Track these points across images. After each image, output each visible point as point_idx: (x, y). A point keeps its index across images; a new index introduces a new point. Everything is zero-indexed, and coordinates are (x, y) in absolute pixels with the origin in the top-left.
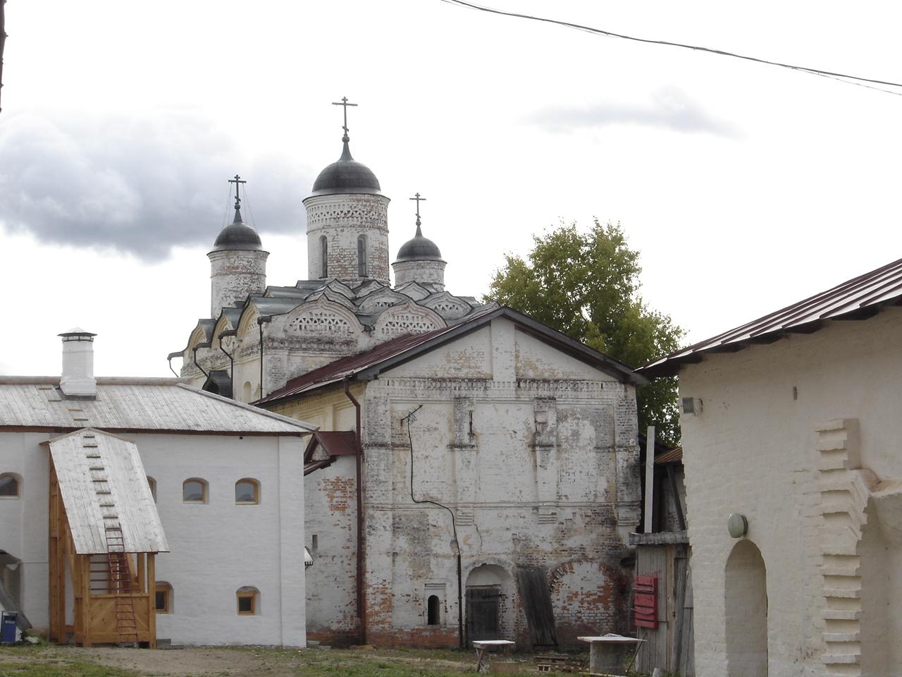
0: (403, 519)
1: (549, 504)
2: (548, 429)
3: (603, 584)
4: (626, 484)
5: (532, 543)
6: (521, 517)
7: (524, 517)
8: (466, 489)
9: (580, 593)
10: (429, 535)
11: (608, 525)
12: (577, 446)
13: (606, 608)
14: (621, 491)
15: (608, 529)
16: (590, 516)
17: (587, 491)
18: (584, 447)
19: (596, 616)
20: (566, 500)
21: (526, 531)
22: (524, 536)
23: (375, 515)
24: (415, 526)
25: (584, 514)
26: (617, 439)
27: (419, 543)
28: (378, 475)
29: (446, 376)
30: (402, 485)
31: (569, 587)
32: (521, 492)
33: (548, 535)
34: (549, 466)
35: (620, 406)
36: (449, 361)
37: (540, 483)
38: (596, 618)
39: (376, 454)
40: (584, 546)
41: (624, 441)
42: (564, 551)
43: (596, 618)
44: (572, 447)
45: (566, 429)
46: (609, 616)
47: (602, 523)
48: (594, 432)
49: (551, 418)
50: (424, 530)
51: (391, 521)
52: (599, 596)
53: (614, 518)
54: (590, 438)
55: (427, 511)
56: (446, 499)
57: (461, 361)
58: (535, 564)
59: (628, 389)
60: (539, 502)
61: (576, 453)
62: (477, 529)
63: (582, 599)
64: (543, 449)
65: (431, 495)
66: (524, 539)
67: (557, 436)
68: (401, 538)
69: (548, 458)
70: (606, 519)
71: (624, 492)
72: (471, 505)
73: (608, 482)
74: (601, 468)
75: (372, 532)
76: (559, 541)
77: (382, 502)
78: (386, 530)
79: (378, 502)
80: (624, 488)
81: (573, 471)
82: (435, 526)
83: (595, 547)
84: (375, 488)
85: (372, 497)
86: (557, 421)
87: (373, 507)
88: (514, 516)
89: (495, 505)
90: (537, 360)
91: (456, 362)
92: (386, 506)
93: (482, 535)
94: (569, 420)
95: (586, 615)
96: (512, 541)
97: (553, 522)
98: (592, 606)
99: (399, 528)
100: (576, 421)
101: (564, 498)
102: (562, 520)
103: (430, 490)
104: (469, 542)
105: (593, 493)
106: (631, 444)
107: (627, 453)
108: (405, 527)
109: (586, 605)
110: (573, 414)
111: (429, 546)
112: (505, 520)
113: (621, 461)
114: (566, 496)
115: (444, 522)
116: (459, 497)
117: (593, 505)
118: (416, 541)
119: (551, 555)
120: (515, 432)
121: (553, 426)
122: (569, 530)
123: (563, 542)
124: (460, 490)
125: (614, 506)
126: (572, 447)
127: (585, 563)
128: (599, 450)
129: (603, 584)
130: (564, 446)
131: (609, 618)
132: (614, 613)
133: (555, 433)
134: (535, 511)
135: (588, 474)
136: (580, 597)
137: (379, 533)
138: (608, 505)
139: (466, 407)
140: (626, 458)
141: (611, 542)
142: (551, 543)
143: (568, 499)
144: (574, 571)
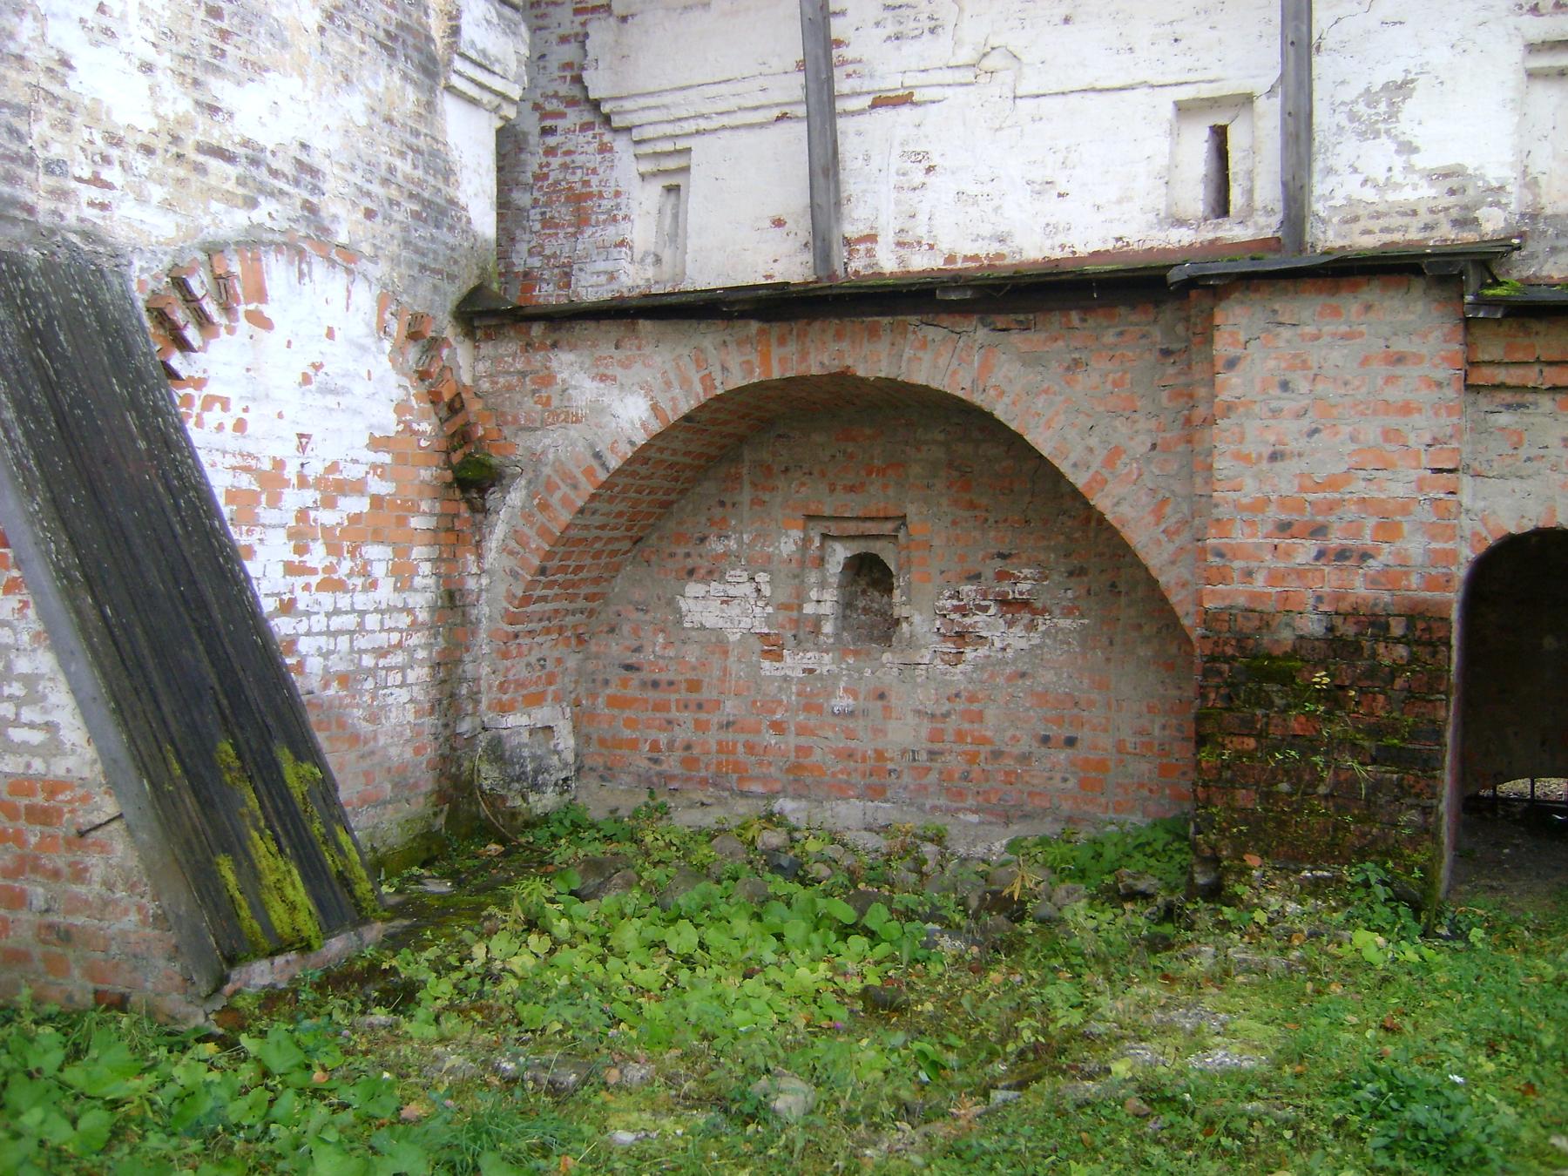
3: (390, 424)
9: (291, 472)
13: (402, 575)
19: (361, 624)
31: (240, 426)
38: (362, 643)
40: (316, 160)
42: (219, 153)
43: (362, 643)
46: (415, 626)
52: (377, 501)
58: (44, 206)
63: (303, 514)
83: (357, 178)
95: (318, 623)
98: (346, 566)
109: (317, 556)
119: (141, 163)
123: (221, 90)
127: (319, 269)
129: (390, 424)
131: (416, 639)
132: (433, 609)
136: (293, 499)
141: (419, 173)
142: (147, 68)
144: (268, 311)
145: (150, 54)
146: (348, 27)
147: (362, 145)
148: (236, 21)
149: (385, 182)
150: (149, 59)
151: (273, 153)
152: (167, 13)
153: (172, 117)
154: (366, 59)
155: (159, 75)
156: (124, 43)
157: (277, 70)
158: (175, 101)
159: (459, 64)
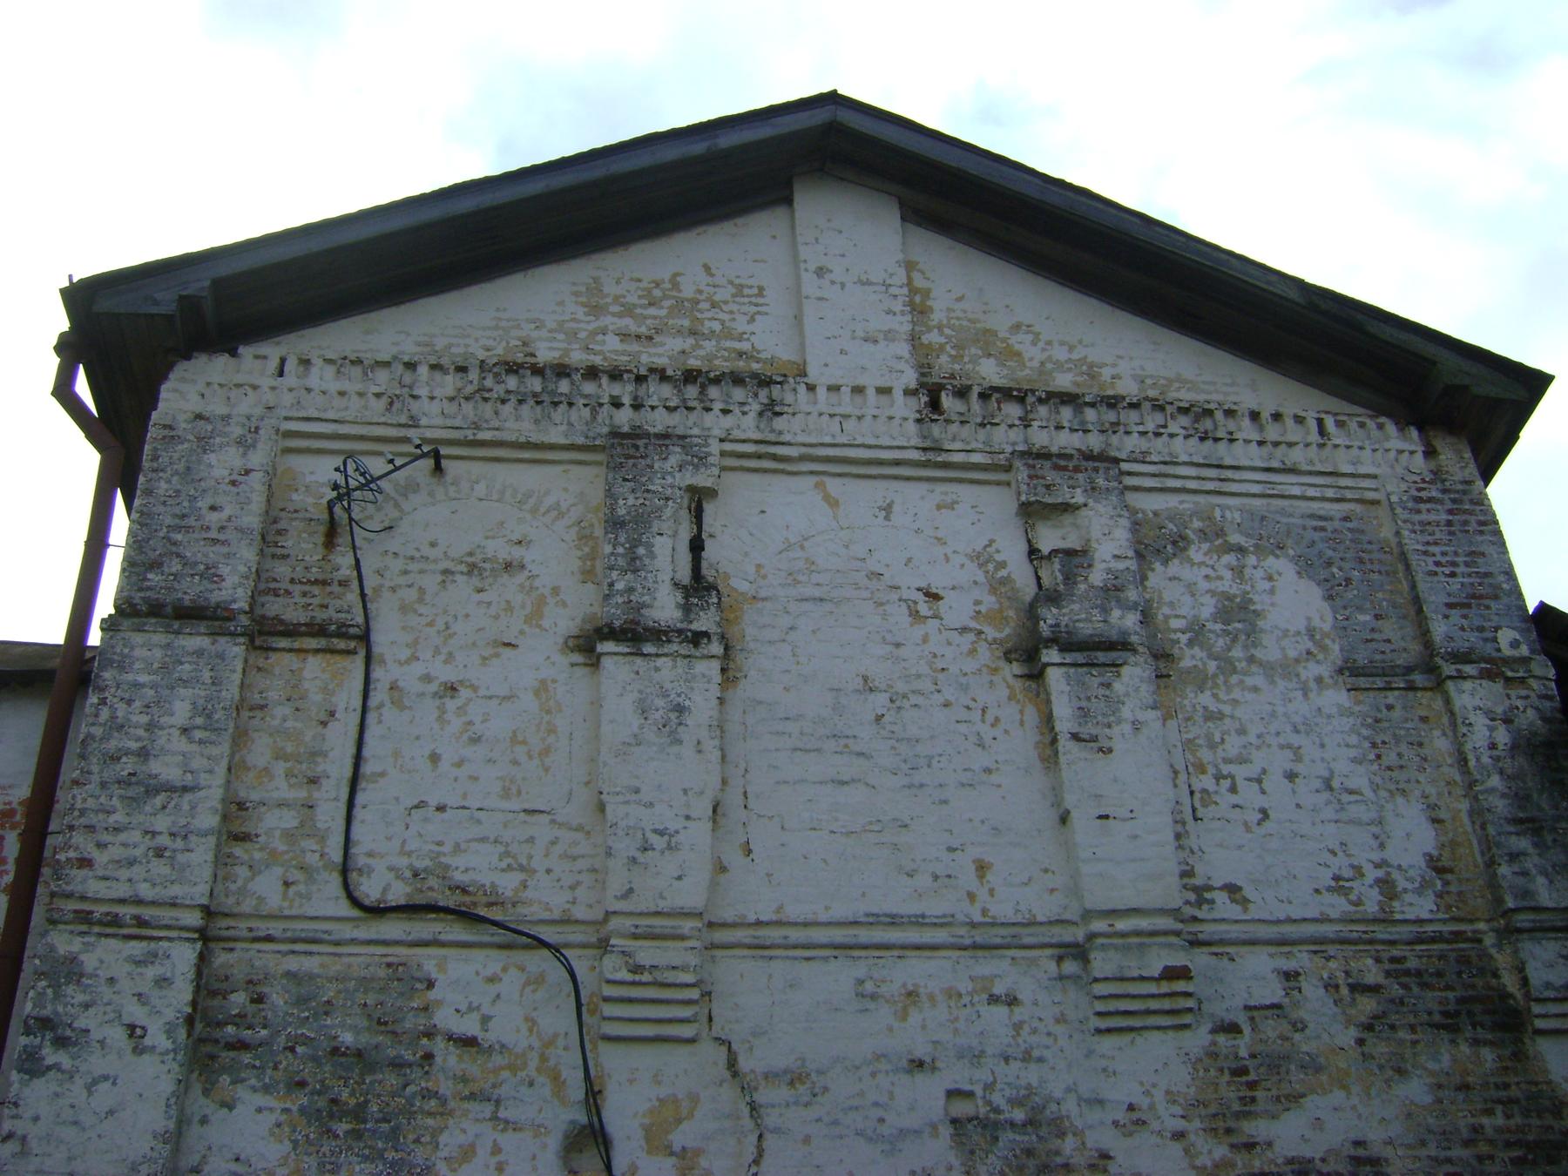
0: (278, 998)
1: (1144, 923)
2: (1097, 577)
4: (1530, 825)
5: (1069, 1144)
6: (994, 999)
7: (1012, 1001)
8: (658, 842)
10: (427, 1094)
11: (1481, 1033)
12: (1251, 660)
14: (1514, 857)
15: (1488, 1054)
16: (1374, 989)
17: (1340, 864)
18: (1287, 669)
20: (1234, 911)
21: (1032, 1075)
22: (1015, 1102)
23: (89, 961)
24: (347, 1038)
25: (1341, 978)
26: (1439, 629)
27: (357, 1135)
28: (144, 754)
29: (577, 357)
30: (289, 820)
32: (982, 868)
33: (1159, 1095)
34: (1119, 736)
35: (1419, 500)
36: (596, 310)
37: (1082, 820)
39: (158, 653)
40: (1376, 1150)
41: (1473, 637)
44: (1228, 667)
45: (1186, 590)
47: (1449, 1023)
48: (1325, 607)
49: (1106, 536)
50: (397, 1065)
51: (181, 995)
53: (1505, 996)
54: (1311, 631)
55: (428, 961)
56: (544, 899)
57: (652, 311)
59: (1438, 443)
60: (1088, 915)
61: (1255, 689)
62: (732, 1064)
64: (1079, 657)
65: (459, 877)
66: (1019, 1115)
67: (1147, 617)
68: (249, 1099)
69: (1114, 704)
70: (1461, 1001)
71: (1529, 864)
72: (687, 926)
73: (1436, 821)
74: (1390, 758)
75: (50, 1056)
76: (1223, 1123)
77: (145, 891)
78: (139, 1050)
79: (122, 890)
80: (1523, 843)
81: (1252, 770)
82: (469, 1042)
84: (118, 817)
85: (85, 863)
86: (1140, 556)
87: (84, 917)
88: (952, 994)
89: (838, 935)
90: (1016, 327)
91: (629, 311)
92: (166, 915)
93: (761, 1097)
94: (1196, 553)
96: (946, 1131)
97: (1178, 1018)
99: (242, 1046)
100: (1230, 558)
101: (1221, 897)
102: (1229, 1006)
103: (457, 848)
104: (678, 1138)
105: (1372, 874)
106: (1507, 652)
107: (1498, 686)
108: (282, 1040)
110: (1214, 533)
111: (419, 1155)
112: (903, 1016)
113: (1480, 721)
114: (1232, 889)
115: (531, 1022)
116: (616, 884)
117: (1382, 932)
118: (342, 1127)
120: (934, 597)
121: (1121, 565)
122: (1276, 1064)
123: (1257, 1128)
124: (625, 847)
125: (1489, 940)
126: (1228, 667)
128: (1363, 682)
130: (1190, 658)
133: (1132, 594)
134: (1070, 967)
135: (1331, 789)
137: (96, 1063)
138: (1457, 936)
139: (671, 474)
140: (1499, 710)
141: (1518, 1120)
142: (1179, 1136)
143: (1245, 902)
145: (1181, 1124)
146: (1393, 1027)
147: (1431, 1121)
148: (1262, 1070)
149: (1467, 1143)
150: (1180, 1128)
151: (1323, 1160)
152: (1193, 1089)
153: (1209, 1164)
154: (1419, 1047)
155: (1192, 1137)
156: (1155, 1125)
157: (1313, 1091)
158: (1210, 1152)
159: (1537, 1009)
